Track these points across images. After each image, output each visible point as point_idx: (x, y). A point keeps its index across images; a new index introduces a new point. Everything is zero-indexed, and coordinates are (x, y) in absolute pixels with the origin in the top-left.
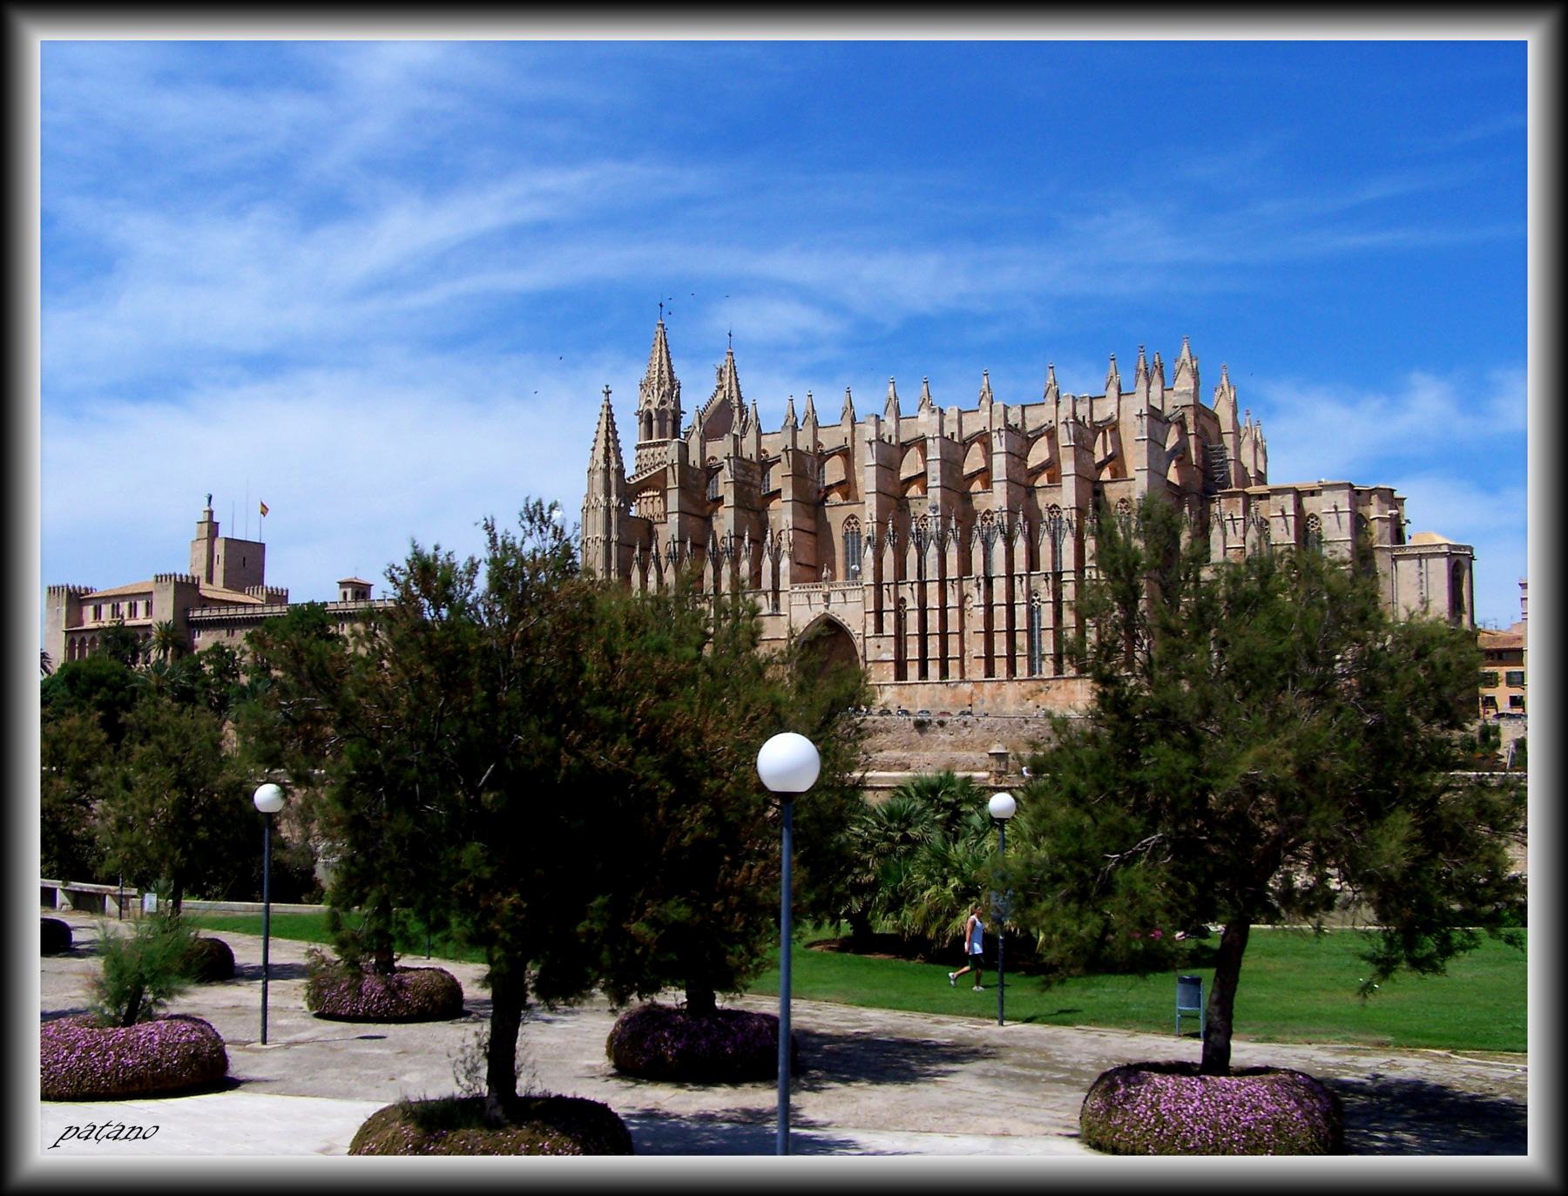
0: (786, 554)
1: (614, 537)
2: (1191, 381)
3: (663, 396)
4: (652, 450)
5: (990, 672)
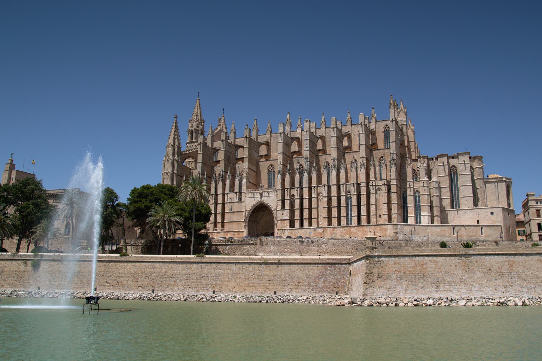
0: (245, 178)
1: (175, 172)
2: (404, 115)
3: (198, 124)
4: (192, 144)
5: (330, 224)
